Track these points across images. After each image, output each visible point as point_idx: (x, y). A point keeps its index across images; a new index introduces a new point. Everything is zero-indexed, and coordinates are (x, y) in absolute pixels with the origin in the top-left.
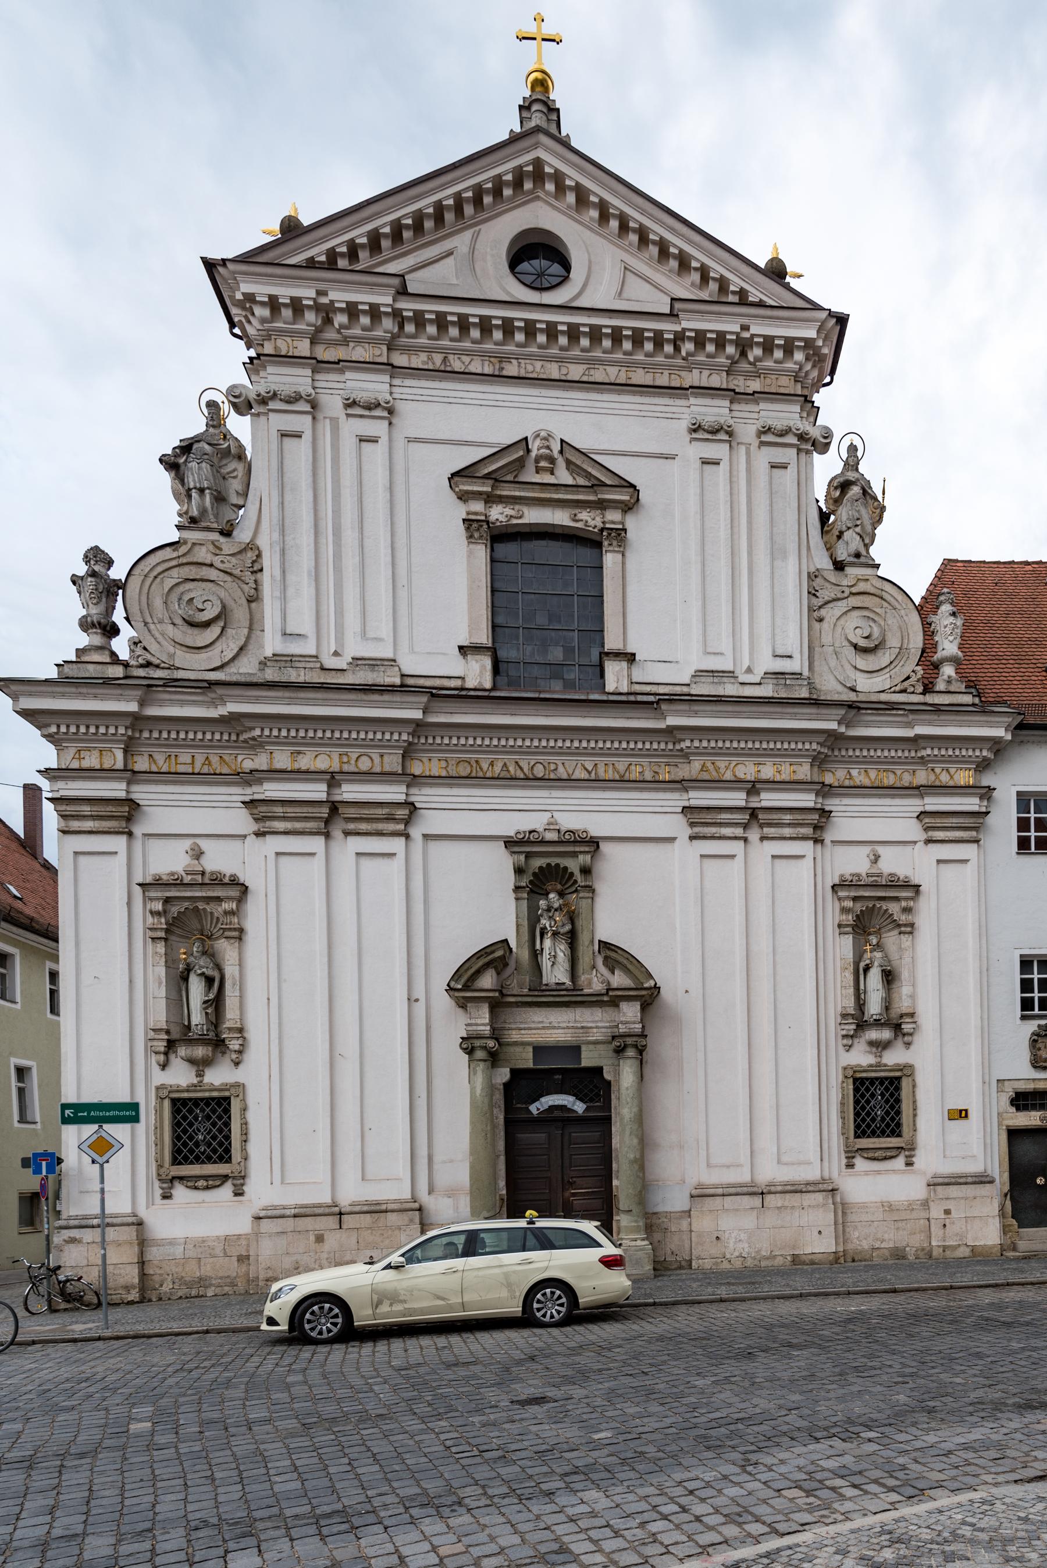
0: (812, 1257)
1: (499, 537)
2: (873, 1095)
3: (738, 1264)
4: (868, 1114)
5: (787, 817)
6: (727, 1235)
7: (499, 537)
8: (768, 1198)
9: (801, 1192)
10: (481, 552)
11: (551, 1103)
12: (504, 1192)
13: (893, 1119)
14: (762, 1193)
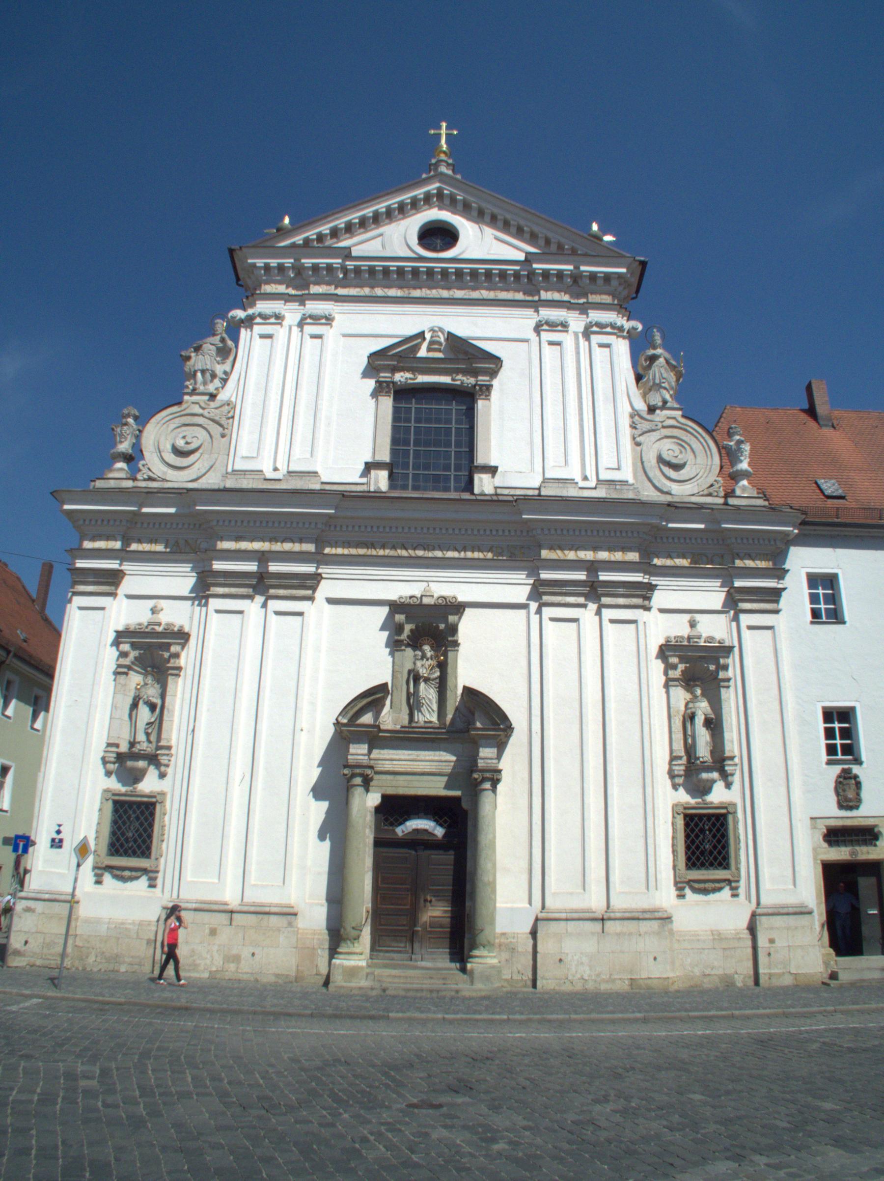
0: (649, 981)
1: (402, 394)
2: (702, 831)
3: (579, 987)
4: (698, 848)
5: (621, 591)
6: (570, 957)
7: (402, 394)
8: (608, 924)
9: (638, 919)
10: (387, 403)
11: (414, 827)
12: (370, 905)
13: (720, 853)
14: (603, 919)
